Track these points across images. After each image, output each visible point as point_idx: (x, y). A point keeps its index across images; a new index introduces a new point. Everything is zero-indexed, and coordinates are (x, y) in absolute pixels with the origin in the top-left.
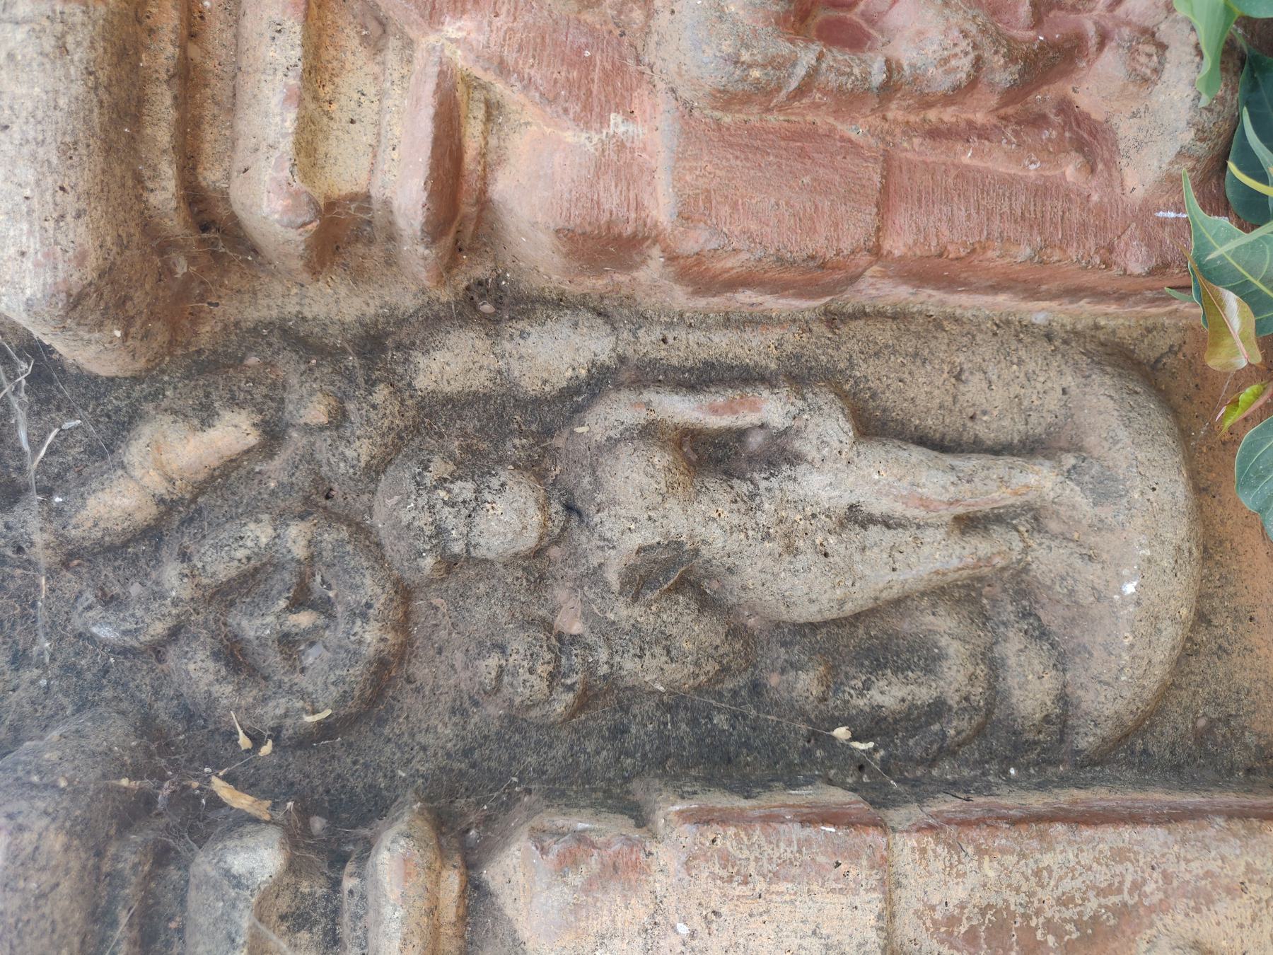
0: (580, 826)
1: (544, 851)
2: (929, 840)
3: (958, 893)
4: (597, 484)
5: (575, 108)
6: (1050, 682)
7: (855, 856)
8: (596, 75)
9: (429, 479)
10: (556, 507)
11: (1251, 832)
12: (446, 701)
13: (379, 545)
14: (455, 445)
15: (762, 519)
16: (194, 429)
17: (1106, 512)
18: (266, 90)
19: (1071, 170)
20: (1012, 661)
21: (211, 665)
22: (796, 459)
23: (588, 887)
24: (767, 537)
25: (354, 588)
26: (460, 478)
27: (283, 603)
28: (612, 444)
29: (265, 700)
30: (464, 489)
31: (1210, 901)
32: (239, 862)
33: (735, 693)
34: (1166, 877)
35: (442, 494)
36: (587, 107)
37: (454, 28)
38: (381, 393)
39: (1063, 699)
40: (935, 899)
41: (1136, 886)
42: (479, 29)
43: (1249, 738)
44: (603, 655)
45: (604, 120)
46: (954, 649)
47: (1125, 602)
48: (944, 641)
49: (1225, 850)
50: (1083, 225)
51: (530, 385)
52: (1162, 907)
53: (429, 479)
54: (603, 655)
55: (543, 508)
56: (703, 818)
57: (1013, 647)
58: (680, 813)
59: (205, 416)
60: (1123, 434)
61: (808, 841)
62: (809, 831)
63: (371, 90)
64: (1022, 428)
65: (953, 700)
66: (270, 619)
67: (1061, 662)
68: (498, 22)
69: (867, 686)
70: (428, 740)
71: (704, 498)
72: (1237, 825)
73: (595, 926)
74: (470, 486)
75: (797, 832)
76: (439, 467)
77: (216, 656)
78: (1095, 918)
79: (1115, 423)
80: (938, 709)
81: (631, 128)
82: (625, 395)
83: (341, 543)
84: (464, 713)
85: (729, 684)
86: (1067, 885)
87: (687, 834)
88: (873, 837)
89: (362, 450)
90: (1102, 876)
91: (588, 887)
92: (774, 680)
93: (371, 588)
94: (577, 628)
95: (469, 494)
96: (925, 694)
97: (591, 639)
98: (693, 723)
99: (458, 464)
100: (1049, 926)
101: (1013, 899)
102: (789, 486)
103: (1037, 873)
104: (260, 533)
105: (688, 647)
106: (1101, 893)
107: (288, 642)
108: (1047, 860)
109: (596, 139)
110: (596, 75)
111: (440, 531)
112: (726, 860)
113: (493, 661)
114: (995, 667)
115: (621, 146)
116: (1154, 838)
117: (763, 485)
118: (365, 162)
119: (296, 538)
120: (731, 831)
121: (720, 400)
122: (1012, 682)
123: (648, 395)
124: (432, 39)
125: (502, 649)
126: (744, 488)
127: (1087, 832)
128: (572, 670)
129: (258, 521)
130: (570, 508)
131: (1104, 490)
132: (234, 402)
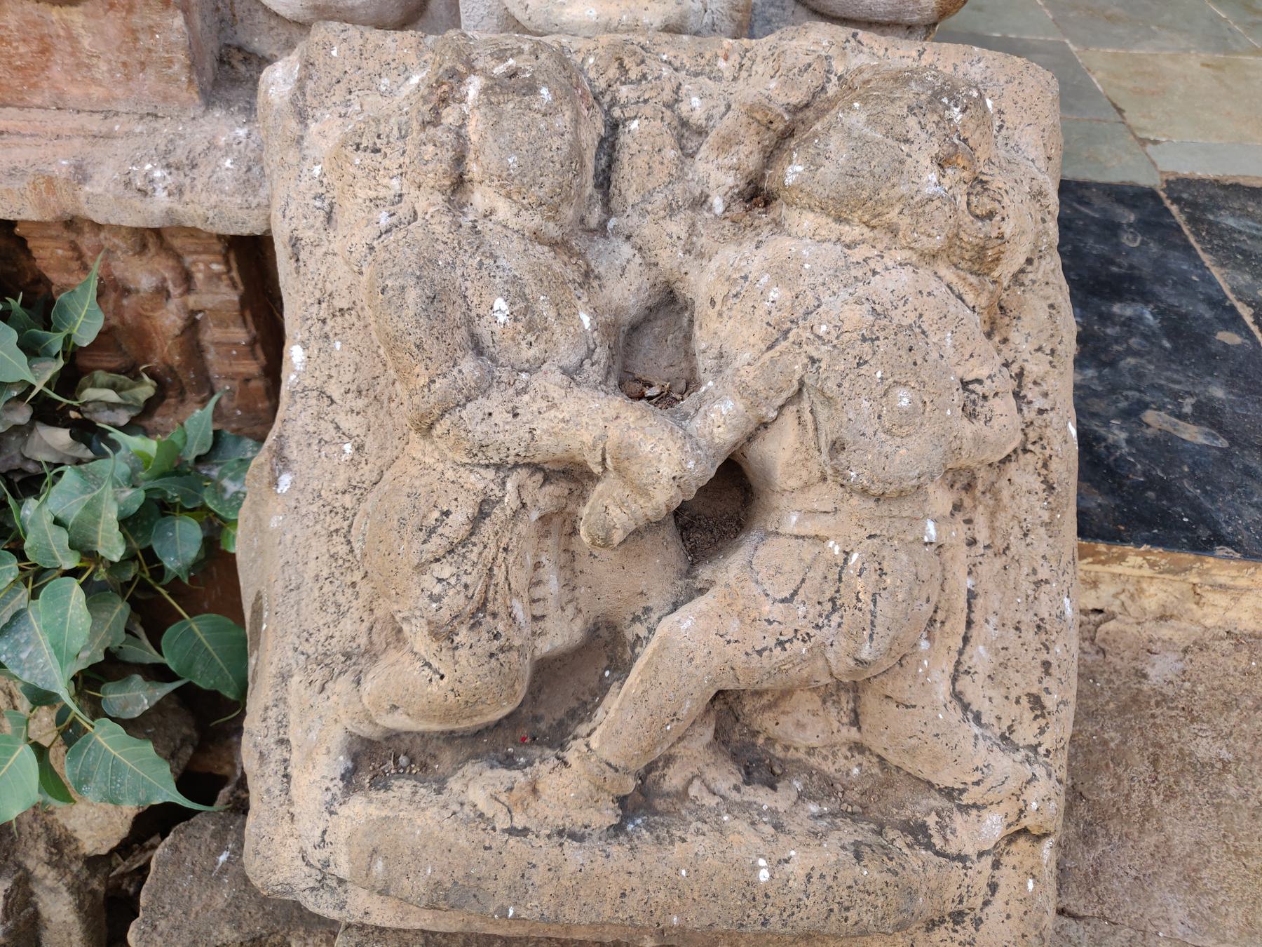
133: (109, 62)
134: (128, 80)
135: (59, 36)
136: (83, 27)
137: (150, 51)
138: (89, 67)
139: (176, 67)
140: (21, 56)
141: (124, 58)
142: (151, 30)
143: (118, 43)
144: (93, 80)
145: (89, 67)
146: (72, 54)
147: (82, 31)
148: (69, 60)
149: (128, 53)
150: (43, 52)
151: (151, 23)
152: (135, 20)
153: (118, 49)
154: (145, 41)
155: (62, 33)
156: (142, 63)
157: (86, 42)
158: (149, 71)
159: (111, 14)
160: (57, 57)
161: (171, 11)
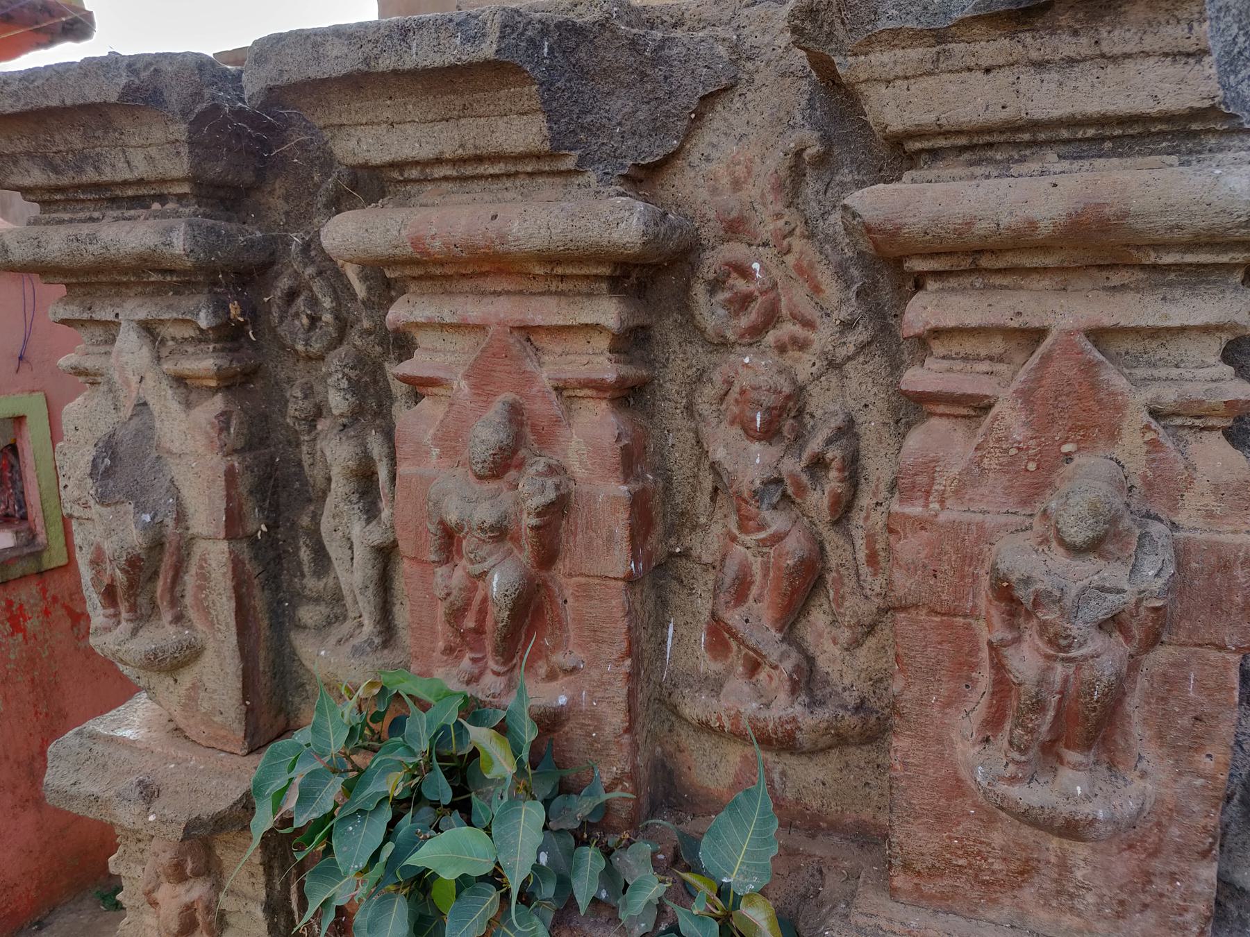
0: (232, 430)
1: (216, 417)
2: (227, 555)
3: (214, 565)
4: (348, 438)
5: (440, 434)
6: (310, 622)
7: (217, 527)
8: (453, 444)
9: (347, 370)
10: (345, 420)
11: (238, 677)
12: (291, 374)
13: (335, 348)
14: (366, 379)
15: (341, 505)
16: (358, 275)
17: (349, 650)
18: (433, 309)
19: (441, 645)
20: (318, 608)
21: (286, 287)
22: (368, 521)
23: (207, 432)
24: (336, 506)
25: (316, 341)
26: (349, 382)
27: (309, 312)
28: (364, 445)
29: (279, 307)
30: (344, 384)
31: (218, 656)
32: (202, 314)
33: (307, 491)
34: (223, 642)
35: (340, 376)
36: (441, 439)
37: (463, 384)
38: (378, 349)
39: (305, 627)
40: (211, 555)
41: (220, 630)
42: (465, 395)
43: (303, 706)
44: (306, 438)
45: (436, 446)
46: (321, 584)
47: (319, 651)
48: (325, 580)
49: (232, 666)
50: (422, 647)
51: (395, 410)
52: (216, 640)
53: (347, 370)
54: (306, 438)
55: (341, 415)
56: (230, 475)
57: (323, 609)
58: (233, 466)
59: (364, 278)
60: (380, 662)
61: (220, 510)
62: (223, 511)
63: (457, 347)
64: (401, 626)
65: (305, 581)
66: (303, 308)
67: (317, 628)
68: (468, 403)
69: (307, 546)
70: (279, 369)
71: (345, 481)
72: (240, 673)
73: (196, 434)
74: (346, 386)
75: (224, 506)
76: (353, 374)
77: (290, 288)
78: (210, 613)
79: (386, 661)
80: (303, 576)
81: (435, 457)
82: (386, 450)
83: (331, 335)
84: (288, 383)
85: (310, 489)
86: (218, 605)
87: (222, 468)
88: (222, 535)
89: (358, 343)
90: (221, 617)
91: (207, 432)
92: (312, 508)
93: (316, 347)
94: (319, 427)
95: (342, 386)
96: (306, 569)
97: (313, 434)
98: (295, 474)
99: (359, 381)
100: (207, 596)
101: (213, 583)
102: (357, 517)
103: (220, 594)
104: (327, 303)
105: (315, 472)
106: (217, 616)
107: (297, 315)
108: (225, 599)
109: (429, 442)
110: (453, 444)
111: (330, 374)
112: (214, 481)
113: (299, 394)
114: (317, 600)
115: (427, 453)
116: (233, 639)
117: (356, 506)
118: (430, 346)
119: (327, 317)
120: (223, 483)
121: (387, 491)
122: (311, 607)
123: (385, 460)
124: (460, 376)
125: (306, 397)
126: (355, 498)
127: (233, 614)
128: (299, 425)
129: (332, 302)
130: (344, 426)
131: (356, 651)
132: (369, 289)
133: (1102, 896)
134: (1119, 917)
135: (1048, 862)
136: (1085, 860)
137: (1162, 895)
138: (1072, 897)
139: (1189, 917)
140: (993, 872)
141: (1125, 896)
142: (1173, 877)
143: (1123, 881)
144: (1072, 909)
145: (1072, 897)
146: (1056, 881)
147: (1082, 864)
148: (1048, 885)
149: (1132, 893)
150: (1021, 873)
151: (1173, 868)
152: (1157, 865)
153: (1121, 888)
154: (1160, 885)
155: (1053, 859)
156: (1145, 906)
157: (1079, 874)
158: (1149, 913)
159: (1126, 854)
160: (1036, 880)
161: (1205, 862)
